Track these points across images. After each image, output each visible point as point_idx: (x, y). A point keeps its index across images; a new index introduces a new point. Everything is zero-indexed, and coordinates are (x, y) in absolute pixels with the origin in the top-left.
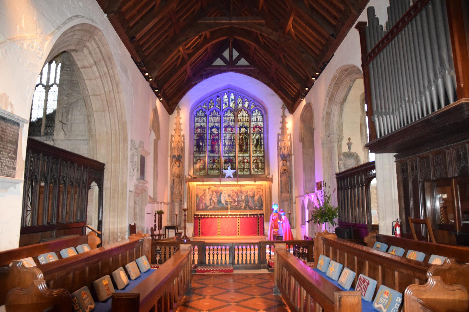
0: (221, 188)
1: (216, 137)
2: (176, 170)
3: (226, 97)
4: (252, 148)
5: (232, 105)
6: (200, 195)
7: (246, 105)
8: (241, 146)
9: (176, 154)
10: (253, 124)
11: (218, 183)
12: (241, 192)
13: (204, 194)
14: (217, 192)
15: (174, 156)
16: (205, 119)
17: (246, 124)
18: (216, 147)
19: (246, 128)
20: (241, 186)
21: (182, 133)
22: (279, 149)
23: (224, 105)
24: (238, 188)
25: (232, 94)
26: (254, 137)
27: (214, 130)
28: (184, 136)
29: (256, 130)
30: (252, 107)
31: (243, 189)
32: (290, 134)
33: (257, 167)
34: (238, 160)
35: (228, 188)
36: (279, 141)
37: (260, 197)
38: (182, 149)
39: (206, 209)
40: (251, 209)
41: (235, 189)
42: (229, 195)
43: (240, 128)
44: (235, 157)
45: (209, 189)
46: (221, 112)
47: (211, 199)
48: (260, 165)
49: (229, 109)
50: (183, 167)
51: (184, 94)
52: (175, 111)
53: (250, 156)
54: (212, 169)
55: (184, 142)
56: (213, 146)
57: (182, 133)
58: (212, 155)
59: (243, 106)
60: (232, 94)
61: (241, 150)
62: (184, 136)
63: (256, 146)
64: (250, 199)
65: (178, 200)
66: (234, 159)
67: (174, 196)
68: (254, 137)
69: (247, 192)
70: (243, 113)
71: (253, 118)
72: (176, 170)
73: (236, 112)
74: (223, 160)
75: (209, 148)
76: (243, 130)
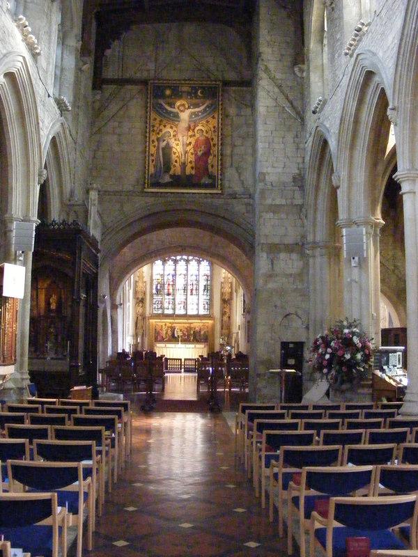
0: (175, 325)
2: (140, 310)
6: (158, 330)
9: (140, 297)
11: (172, 321)
12: (191, 328)
13: (161, 330)
15: (138, 298)
21: (145, 280)
22: (222, 294)
24: (188, 325)
31: (192, 326)
35: (180, 325)
36: (222, 288)
39: (162, 340)
41: (186, 325)
45: (165, 325)
47: (167, 333)
50: (145, 308)
57: (145, 280)
61: (192, 294)
62: (145, 282)
64: (198, 335)
65: (141, 334)
67: (138, 330)
69: (195, 329)
72: (140, 310)
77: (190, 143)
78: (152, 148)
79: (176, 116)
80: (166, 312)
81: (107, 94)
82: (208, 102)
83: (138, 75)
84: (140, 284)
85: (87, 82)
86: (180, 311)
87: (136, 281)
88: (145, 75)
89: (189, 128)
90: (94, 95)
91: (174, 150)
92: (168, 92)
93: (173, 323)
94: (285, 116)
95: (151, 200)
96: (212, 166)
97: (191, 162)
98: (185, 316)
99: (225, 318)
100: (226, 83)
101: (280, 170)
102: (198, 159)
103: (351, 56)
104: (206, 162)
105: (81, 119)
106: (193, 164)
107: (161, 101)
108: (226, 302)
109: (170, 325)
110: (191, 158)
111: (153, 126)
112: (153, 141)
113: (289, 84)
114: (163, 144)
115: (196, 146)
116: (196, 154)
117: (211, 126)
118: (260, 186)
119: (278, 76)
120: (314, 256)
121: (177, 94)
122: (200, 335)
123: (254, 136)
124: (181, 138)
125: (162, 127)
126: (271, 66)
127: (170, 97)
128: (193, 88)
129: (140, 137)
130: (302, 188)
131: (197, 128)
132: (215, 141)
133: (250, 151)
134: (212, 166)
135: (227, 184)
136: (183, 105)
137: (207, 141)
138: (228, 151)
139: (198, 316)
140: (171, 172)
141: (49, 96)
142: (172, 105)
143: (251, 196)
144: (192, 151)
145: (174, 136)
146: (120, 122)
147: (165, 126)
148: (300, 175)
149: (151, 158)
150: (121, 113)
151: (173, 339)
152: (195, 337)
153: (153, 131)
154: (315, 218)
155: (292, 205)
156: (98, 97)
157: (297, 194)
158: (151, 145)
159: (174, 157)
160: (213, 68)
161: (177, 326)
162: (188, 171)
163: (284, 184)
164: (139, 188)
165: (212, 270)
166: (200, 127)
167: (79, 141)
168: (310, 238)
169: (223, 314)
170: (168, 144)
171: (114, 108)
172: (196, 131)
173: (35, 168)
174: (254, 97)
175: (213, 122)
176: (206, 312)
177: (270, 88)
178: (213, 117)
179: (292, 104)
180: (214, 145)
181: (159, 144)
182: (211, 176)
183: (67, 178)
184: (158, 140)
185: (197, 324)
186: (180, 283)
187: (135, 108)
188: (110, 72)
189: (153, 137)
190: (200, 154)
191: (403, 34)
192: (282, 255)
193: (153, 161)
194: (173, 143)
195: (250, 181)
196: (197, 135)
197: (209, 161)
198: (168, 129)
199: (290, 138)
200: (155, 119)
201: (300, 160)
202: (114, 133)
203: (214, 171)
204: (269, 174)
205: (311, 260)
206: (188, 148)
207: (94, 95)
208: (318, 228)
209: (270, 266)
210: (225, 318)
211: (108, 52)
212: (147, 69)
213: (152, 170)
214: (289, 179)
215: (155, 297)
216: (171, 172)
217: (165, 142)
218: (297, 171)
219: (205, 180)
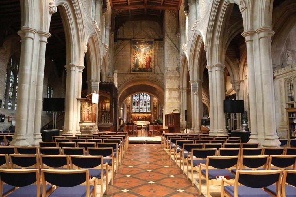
2: (128, 111)
4: (147, 105)
8: (144, 105)
9: (128, 106)
10: (148, 99)
11: (138, 114)
12: (144, 116)
15: (128, 107)
16: (135, 97)
17: (146, 99)
22: (154, 105)
26: (148, 102)
27: (138, 100)
33: (148, 110)
34: (144, 108)
38: (130, 105)
39: (135, 120)
41: (143, 115)
44: (143, 107)
46: (140, 96)
49: (142, 95)
53: (147, 107)
54: (137, 110)
55: (130, 104)
56: (137, 104)
58: (137, 107)
59: (145, 94)
63: (148, 105)
68: (148, 102)
70: (145, 96)
71: (148, 97)
72: (128, 111)
73: (143, 96)
74: (140, 108)
76: (145, 100)
77: (144, 58)
78: (133, 60)
79: (140, 50)
80: (137, 111)
81: (119, 43)
82: (150, 46)
83: (128, 37)
84: (128, 103)
85: (113, 40)
88: (130, 37)
89: (144, 54)
90: (115, 44)
91: (139, 60)
92: (137, 43)
94: (173, 50)
95: (133, 76)
96: (151, 65)
97: (145, 64)
99: (155, 113)
100: (155, 40)
101: (172, 66)
102: (147, 63)
103: (194, 31)
104: (150, 64)
105: (111, 51)
106: (145, 65)
107: (135, 45)
110: (145, 63)
111: (133, 53)
112: (133, 58)
113: (175, 40)
114: (136, 59)
115: (146, 59)
116: (146, 62)
117: (151, 53)
118: (166, 71)
119: (171, 37)
120: (182, 92)
121: (140, 43)
123: (164, 56)
124: (142, 57)
125: (136, 53)
126: (169, 34)
127: (138, 44)
128: (145, 41)
129: (130, 57)
130: (179, 71)
131: (147, 54)
132: (152, 57)
133: (163, 61)
134: (151, 65)
135: (156, 71)
136: (142, 47)
137: (150, 58)
138: (156, 61)
140: (139, 67)
141: (102, 44)
142: (138, 46)
143: (163, 74)
144: (145, 61)
145: (140, 56)
146: (123, 52)
147: (137, 53)
148: (178, 68)
149: (133, 63)
150: (123, 49)
151: (139, 119)
153: (133, 55)
154: (183, 81)
155: (176, 77)
156: (116, 44)
157: (177, 73)
158: (133, 59)
159: (140, 63)
160: (151, 35)
161: (140, 116)
162: (144, 67)
163: (173, 71)
164: (129, 72)
165: (151, 98)
166: (147, 53)
167: (111, 58)
168: (181, 87)
170: (138, 58)
171: (121, 47)
172: (146, 54)
173: (99, 66)
174: (164, 44)
175: (151, 52)
176: (149, 111)
177: (169, 41)
178: (151, 50)
179: (175, 45)
180: (152, 59)
181: (135, 59)
182: (151, 69)
183: (108, 69)
184: (135, 57)
185: (146, 115)
186: (141, 102)
187: (128, 48)
188: (120, 36)
189: (133, 57)
190: (147, 61)
191: (209, 24)
192: (173, 92)
193: (133, 64)
194: (139, 58)
195: (162, 70)
196: (147, 56)
197: (150, 64)
198: (138, 54)
199: (175, 56)
200: (134, 51)
201: (178, 63)
202: (121, 56)
203: (152, 67)
204: (168, 67)
205: (182, 93)
206: (144, 60)
207: (115, 44)
208: (184, 84)
209: (169, 95)
210: (155, 113)
211: (119, 30)
212: (131, 35)
213: (133, 67)
214: (175, 69)
215: (133, 107)
216: (139, 67)
217: (137, 58)
218: (177, 66)
219: (149, 70)
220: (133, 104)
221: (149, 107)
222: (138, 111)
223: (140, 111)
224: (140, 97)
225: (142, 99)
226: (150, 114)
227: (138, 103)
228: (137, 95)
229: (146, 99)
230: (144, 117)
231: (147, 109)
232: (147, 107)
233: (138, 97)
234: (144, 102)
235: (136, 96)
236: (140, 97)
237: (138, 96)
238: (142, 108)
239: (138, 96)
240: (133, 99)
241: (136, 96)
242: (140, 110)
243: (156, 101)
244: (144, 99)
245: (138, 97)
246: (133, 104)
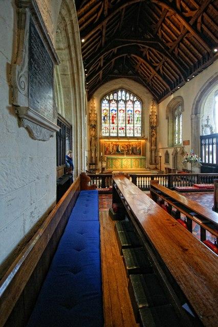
0: (118, 143)
1: (114, 116)
2: (93, 133)
3: (119, 93)
4: (135, 122)
5: (124, 98)
7: (132, 98)
8: (129, 120)
9: (93, 124)
11: (118, 140)
13: (109, 146)
14: (116, 145)
16: (108, 105)
17: (132, 109)
18: (115, 121)
19: (131, 111)
20: (129, 142)
21: (96, 112)
22: (151, 123)
23: (119, 98)
25: (124, 92)
27: (114, 112)
28: (97, 114)
29: (137, 112)
30: (135, 99)
31: (131, 144)
32: (156, 115)
34: (127, 128)
37: (140, 148)
38: (96, 122)
39: (110, 153)
40: (134, 154)
41: (126, 144)
42: (123, 147)
43: (128, 111)
44: (126, 127)
46: (117, 102)
48: (139, 132)
51: (96, 90)
52: (91, 100)
53: (134, 127)
56: (113, 120)
58: (113, 125)
59: (130, 99)
60: (124, 92)
61: (129, 123)
62: (97, 114)
66: (124, 128)
70: (130, 103)
71: (135, 106)
72: (93, 133)
73: (126, 102)
75: (111, 121)
80: (112, 135)
84: (93, 115)
86: (122, 134)
87: (90, 113)
93: (117, 142)
98: (126, 137)
99: (153, 139)
108: (154, 128)
109: (115, 143)
122: (136, 150)
139: (134, 138)
152: (133, 151)
161: (120, 144)
169: (152, 136)
176: (139, 135)
185: (133, 142)
186: (121, 115)
210: (153, 139)
215: (103, 125)
220: (104, 119)
221: (138, 125)
222: (115, 135)
223: (119, 135)
224: (117, 104)
225: (124, 109)
226: (143, 141)
227: (115, 117)
228: (112, 100)
229: (132, 109)
230: (128, 146)
231: (135, 129)
232: (134, 127)
233: (113, 105)
234: (127, 116)
235: (109, 101)
236: (117, 104)
237: (113, 102)
238: (123, 129)
239: (113, 102)
240: (103, 108)
241: (109, 101)
242: (119, 131)
243: (156, 114)
244: (127, 109)
245: (113, 105)
246: (104, 119)
